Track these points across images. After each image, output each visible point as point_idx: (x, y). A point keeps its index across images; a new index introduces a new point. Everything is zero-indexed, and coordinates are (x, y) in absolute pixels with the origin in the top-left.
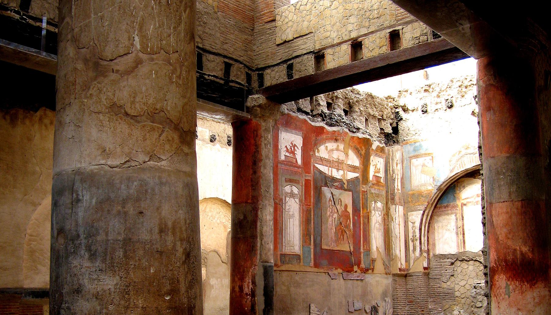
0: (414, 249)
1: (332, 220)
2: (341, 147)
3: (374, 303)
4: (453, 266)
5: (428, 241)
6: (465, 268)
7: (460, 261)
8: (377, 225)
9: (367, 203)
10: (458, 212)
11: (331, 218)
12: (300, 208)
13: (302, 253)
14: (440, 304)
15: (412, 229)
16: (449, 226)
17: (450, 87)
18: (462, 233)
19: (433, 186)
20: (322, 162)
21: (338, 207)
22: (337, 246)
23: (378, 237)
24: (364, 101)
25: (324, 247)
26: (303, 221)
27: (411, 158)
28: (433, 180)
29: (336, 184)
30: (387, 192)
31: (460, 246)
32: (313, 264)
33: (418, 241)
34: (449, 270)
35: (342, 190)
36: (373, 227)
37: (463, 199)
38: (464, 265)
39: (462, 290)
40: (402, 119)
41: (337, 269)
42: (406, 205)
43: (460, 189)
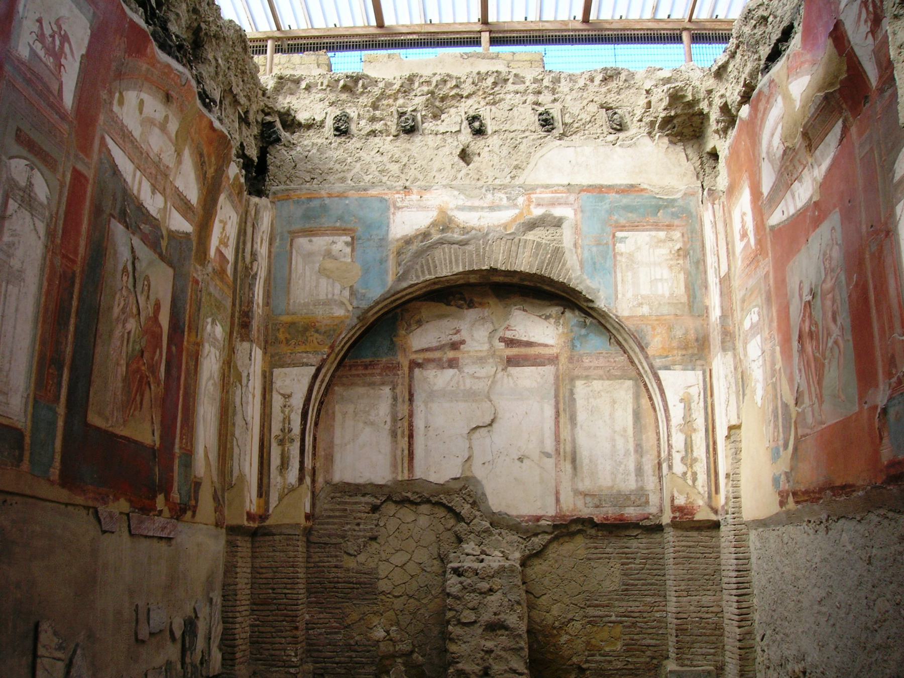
1: (123, 336)
2: (173, 126)
3: (189, 611)
4: (377, 515)
5: (314, 447)
6: (409, 520)
7: (396, 502)
8: (211, 388)
9: (198, 315)
10: (400, 381)
11: (120, 326)
12: (44, 258)
13: (29, 423)
14: (337, 611)
15: (283, 412)
17: (405, 92)
18: (407, 433)
19: (350, 308)
20: (124, 141)
21: (142, 300)
23: (209, 417)
24: (228, 45)
25: (94, 419)
26: (46, 310)
27: (294, 234)
29: (146, 228)
30: (234, 305)
31: (400, 469)
32: (57, 472)
33: (297, 444)
34: (365, 523)
35: (155, 251)
36: (203, 388)
37: (414, 349)
38: (407, 514)
39: (398, 577)
40: (278, 140)
42: (271, 350)
43: (409, 325)
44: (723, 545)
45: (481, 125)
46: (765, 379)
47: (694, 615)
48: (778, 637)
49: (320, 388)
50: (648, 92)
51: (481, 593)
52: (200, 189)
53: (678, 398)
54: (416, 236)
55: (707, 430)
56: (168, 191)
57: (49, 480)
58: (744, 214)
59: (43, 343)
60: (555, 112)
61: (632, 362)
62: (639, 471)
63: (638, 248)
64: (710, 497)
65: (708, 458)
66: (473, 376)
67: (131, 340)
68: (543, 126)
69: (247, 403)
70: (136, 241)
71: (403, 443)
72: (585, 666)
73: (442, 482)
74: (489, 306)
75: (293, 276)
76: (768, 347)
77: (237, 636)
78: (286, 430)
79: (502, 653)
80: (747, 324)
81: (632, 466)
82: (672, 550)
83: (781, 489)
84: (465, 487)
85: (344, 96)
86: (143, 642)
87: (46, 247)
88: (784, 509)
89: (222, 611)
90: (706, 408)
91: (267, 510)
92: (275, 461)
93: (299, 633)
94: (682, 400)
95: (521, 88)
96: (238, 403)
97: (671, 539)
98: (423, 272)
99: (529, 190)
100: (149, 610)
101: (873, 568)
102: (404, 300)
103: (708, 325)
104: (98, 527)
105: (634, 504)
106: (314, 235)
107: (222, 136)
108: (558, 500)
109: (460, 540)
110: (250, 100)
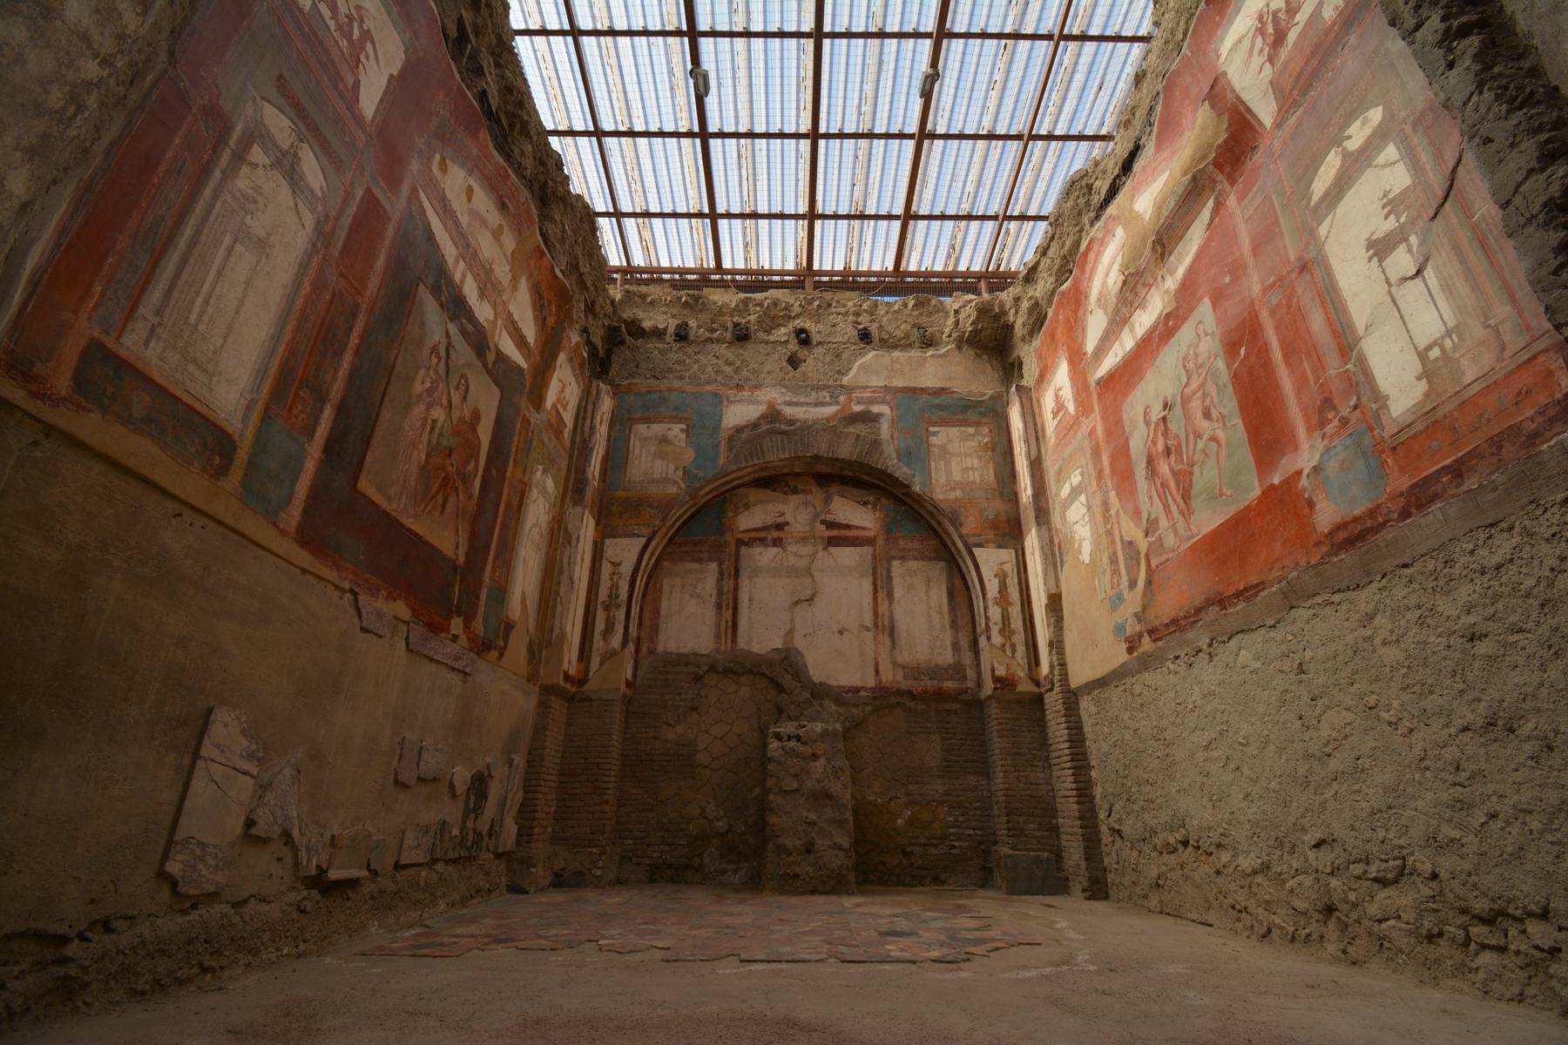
0: (609, 630)
1: (425, 419)
5: (640, 618)
7: (718, 672)
12: (308, 257)
13: (249, 434)
15: (611, 579)
16: (700, 586)
18: (731, 605)
19: (683, 486)
22: (416, 516)
25: (366, 486)
27: (633, 421)
28: (684, 474)
30: (569, 469)
33: (623, 610)
40: (623, 342)
41: (395, 600)
44: (1048, 717)
45: (808, 336)
46: (1094, 532)
47: (1024, 793)
48: (1136, 807)
49: (649, 560)
50: (956, 312)
51: (804, 758)
52: (537, 332)
53: (992, 574)
54: (746, 426)
55: (1022, 605)
56: (500, 308)
57: (275, 525)
58: (1060, 389)
59: (292, 351)
60: (873, 328)
61: (945, 545)
62: (956, 647)
63: (950, 441)
64: (1030, 669)
65: (1025, 631)
66: (796, 555)
67: (437, 431)
68: (862, 339)
69: (575, 563)
70: (453, 329)
71: (728, 615)
72: (908, 850)
73: (763, 652)
74: (811, 492)
75: (631, 456)
76: (1097, 501)
77: (539, 808)
78: (613, 596)
79: (826, 826)
80: (1065, 491)
81: (948, 643)
82: (995, 722)
83: (1129, 633)
84: (786, 658)
85: (685, 312)
86: (407, 787)
87: (314, 245)
88: (1135, 654)
89: (525, 779)
90: (1020, 584)
91: (587, 674)
92: (600, 625)
93: (607, 808)
94: (996, 576)
95: (843, 310)
96: (565, 560)
97: (995, 711)
98: (752, 458)
99: (849, 390)
100: (421, 748)
101: (1311, 676)
102: (733, 485)
103: (1018, 508)
104: (356, 621)
105: (952, 678)
106: (654, 422)
107: (562, 287)
108: (877, 672)
109: (780, 711)
110: (596, 290)
